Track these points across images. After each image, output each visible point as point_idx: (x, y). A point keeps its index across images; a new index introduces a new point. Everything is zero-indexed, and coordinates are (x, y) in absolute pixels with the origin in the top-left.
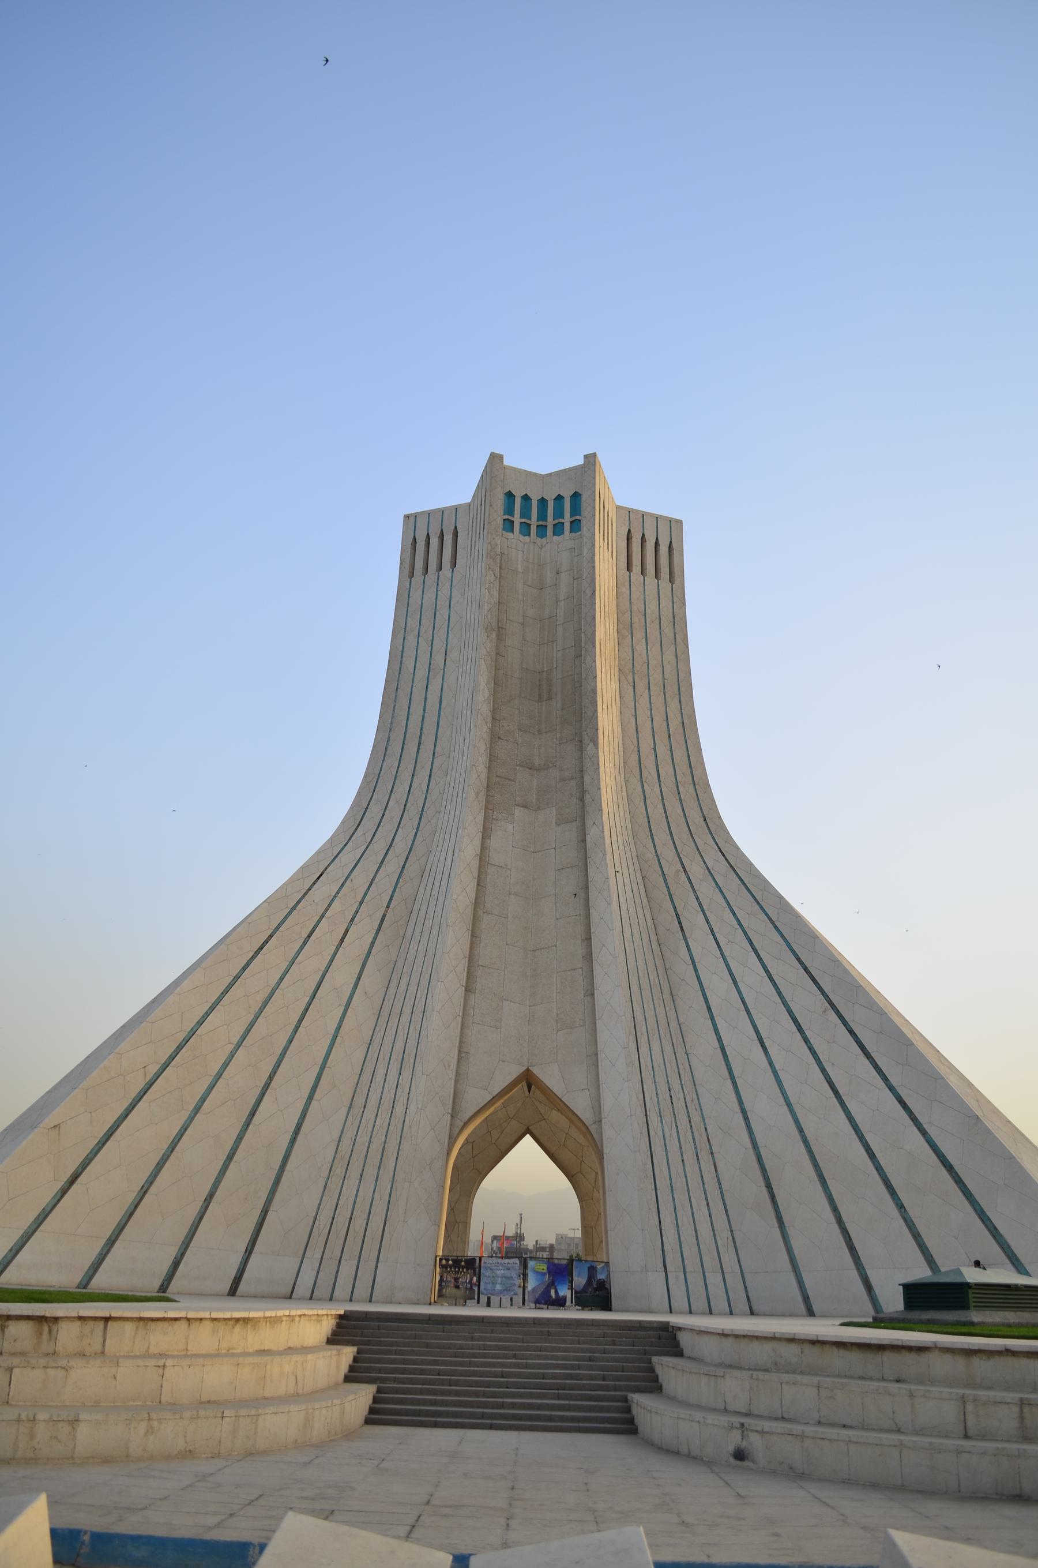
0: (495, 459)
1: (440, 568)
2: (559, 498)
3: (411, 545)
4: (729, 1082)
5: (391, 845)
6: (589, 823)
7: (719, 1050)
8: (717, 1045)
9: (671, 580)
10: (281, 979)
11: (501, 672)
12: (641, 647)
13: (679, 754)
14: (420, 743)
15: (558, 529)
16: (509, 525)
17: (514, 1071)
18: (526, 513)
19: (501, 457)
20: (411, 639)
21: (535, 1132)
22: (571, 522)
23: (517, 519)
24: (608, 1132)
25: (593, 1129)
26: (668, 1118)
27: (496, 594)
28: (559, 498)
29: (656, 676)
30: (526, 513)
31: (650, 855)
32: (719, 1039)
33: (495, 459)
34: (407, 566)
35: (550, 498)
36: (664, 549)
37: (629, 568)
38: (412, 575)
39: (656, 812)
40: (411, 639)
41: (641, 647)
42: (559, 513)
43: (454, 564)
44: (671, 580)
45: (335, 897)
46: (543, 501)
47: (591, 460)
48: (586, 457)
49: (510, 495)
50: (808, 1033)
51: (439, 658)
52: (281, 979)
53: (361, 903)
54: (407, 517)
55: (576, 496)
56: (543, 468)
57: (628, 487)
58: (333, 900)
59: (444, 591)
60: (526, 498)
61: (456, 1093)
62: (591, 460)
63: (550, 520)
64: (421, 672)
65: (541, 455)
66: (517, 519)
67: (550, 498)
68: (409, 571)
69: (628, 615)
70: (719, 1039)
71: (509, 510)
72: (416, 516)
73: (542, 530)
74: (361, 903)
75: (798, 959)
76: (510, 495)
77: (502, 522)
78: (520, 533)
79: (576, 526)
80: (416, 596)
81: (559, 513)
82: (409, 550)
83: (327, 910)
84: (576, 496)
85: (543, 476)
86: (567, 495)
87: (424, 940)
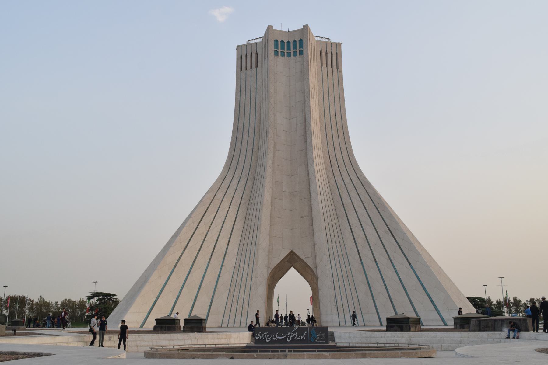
0: (270, 28)
2: (295, 41)
3: (240, 58)
6: (309, 165)
9: (337, 68)
16: (276, 53)
17: (289, 251)
18: (283, 48)
19: (272, 26)
25: (314, 270)
28: (295, 41)
30: (283, 48)
35: (291, 41)
37: (321, 65)
42: (295, 47)
43: (257, 66)
44: (337, 68)
46: (289, 42)
47: (306, 27)
48: (304, 26)
49: (276, 41)
54: (237, 46)
55: (301, 40)
57: (320, 31)
60: (282, 42)
62: (306, 27)
63: (292, 51)
65: (288, 24)
67: (291, 41)
68: (240, 69)
71: (276, 46)
76: (276, 41)
79: (301, 53)
81: (295, 47)
82: (240, 60)
84: (301, 40)
86: (298, 40)
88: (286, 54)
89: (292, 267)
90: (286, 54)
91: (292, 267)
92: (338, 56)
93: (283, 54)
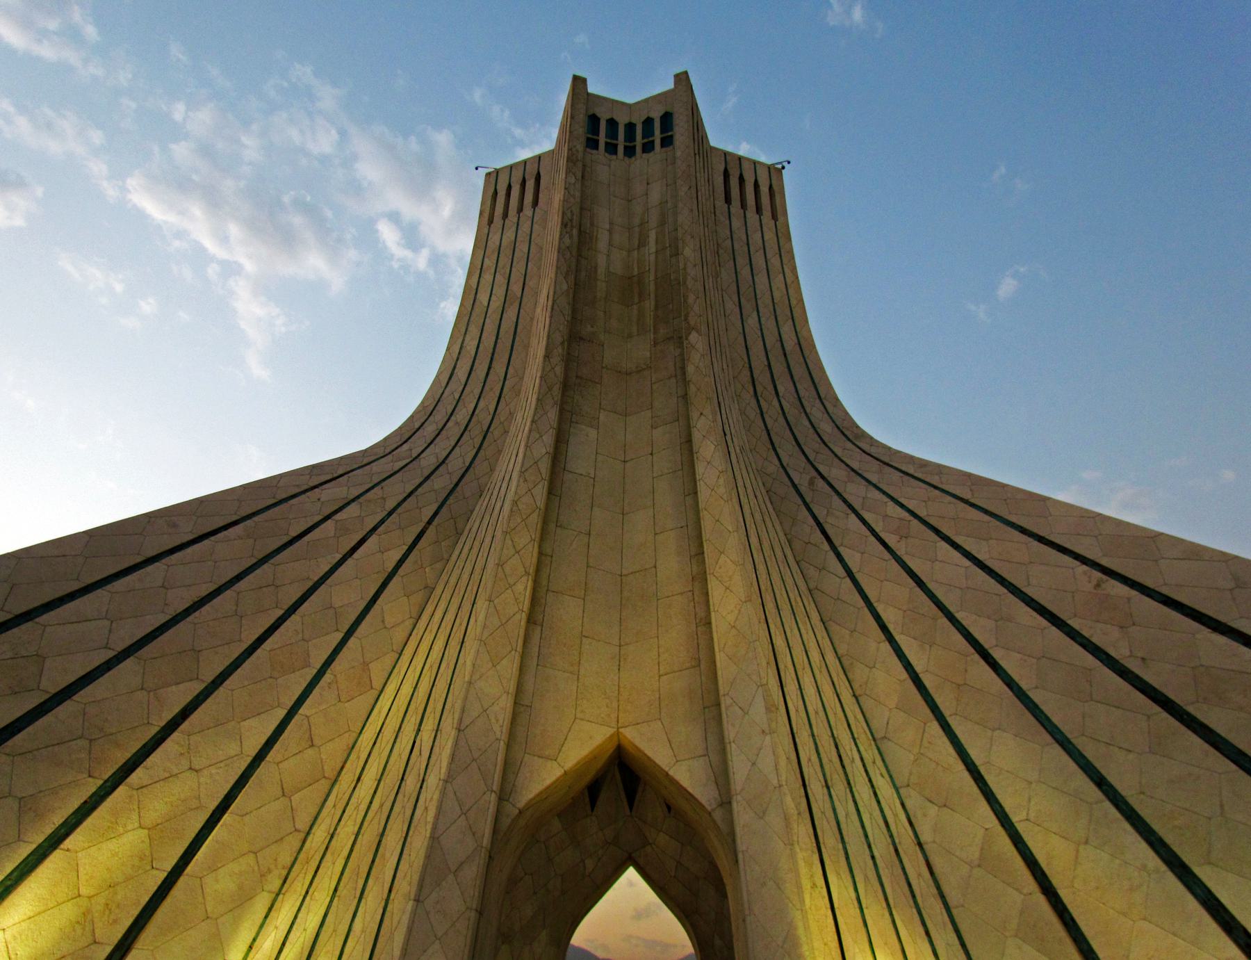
0: (579, 83)
1: (520, 210)
4: (935, 727)
5: (443, 462)
7: (910, 682)
8: (905, 675)
9: (774, 217)
10: (238, 578)
11: (583, 274)
12: (745, 272)
13: (799, 371)
14: (489, 368)
15: (648, 148)
19: (584, 81)
20: (487, 277)
21: (641, 861)
22: (662, 140)
23: (602, 139)
24: (743, 816)
25: (718, 815)
26: (839, 788)
27: (578, 194)
29: (764, 301)
31: (773, 467)
32: (908, 666)
33: (579, 83)
34: (486, 215)
36: (764, 190)
37: (728, 200)
38: (491, 222)
39: (778, 426)
40: (487, 277)
41: (745, 272)
43: (535, 203)
44: (774, 217)
45: (353, 500)
47: (682, 79)
48: (677, 77)
50: (1075, 623)
51: (516, 288)
52: (238, 578)
53: (390, 514)
56: (630, 99)
58: (348, 504)
59: (525, 227)
60: (612, 123)
61: (506, 763)
62: (682, 79)
64: (496, 303)
66: (602, 139)
69: (729, 242)
70: (908, 666)
72: (497, 172)
73: (630, 152)
74: (390, 514)
75: (1024, 531)
77: (583, 140)
78: (606, 151)
80: (494, 239)
83: (336, 512)
85: (629, 106)
86: (656, 115)
87: (472, 557)
88: (621, 149)
89: (631, 873)
90: (621, 149)
91: (631, 873)
92: (775, 192)
93: (611, 149)
